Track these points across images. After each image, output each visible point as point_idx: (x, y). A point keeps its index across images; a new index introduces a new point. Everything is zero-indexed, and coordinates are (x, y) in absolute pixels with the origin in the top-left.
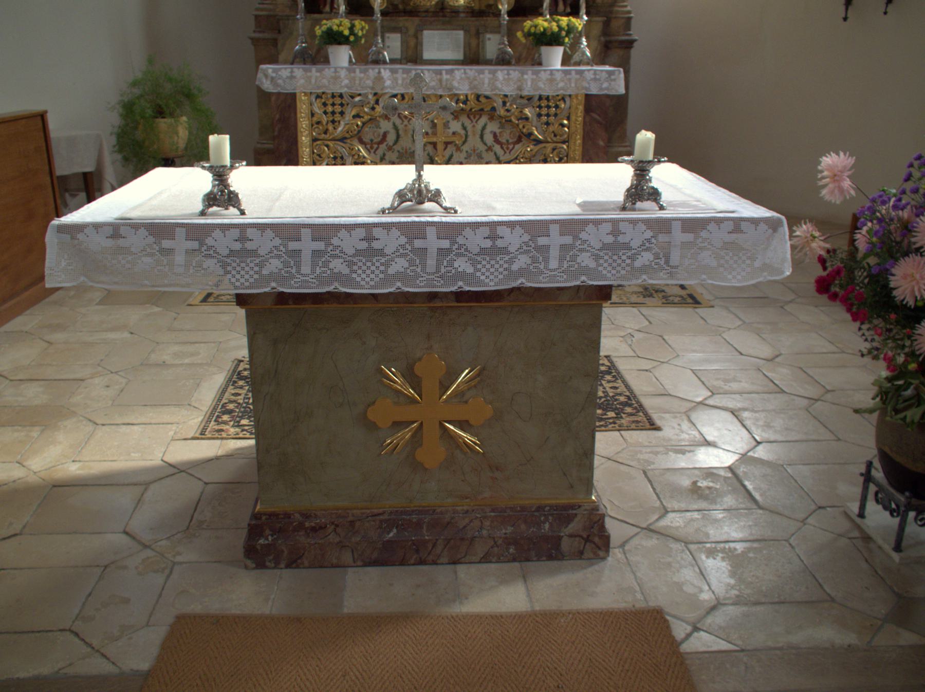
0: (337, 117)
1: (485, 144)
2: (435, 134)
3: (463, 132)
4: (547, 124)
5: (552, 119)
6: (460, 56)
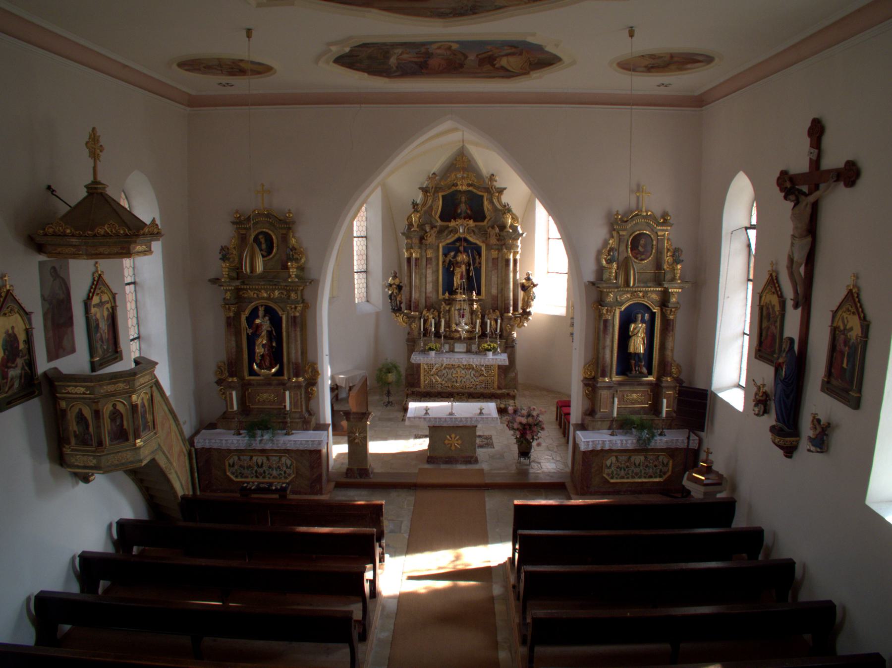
0: (431, 369)
2: (457, 374)
6: (465, 350)
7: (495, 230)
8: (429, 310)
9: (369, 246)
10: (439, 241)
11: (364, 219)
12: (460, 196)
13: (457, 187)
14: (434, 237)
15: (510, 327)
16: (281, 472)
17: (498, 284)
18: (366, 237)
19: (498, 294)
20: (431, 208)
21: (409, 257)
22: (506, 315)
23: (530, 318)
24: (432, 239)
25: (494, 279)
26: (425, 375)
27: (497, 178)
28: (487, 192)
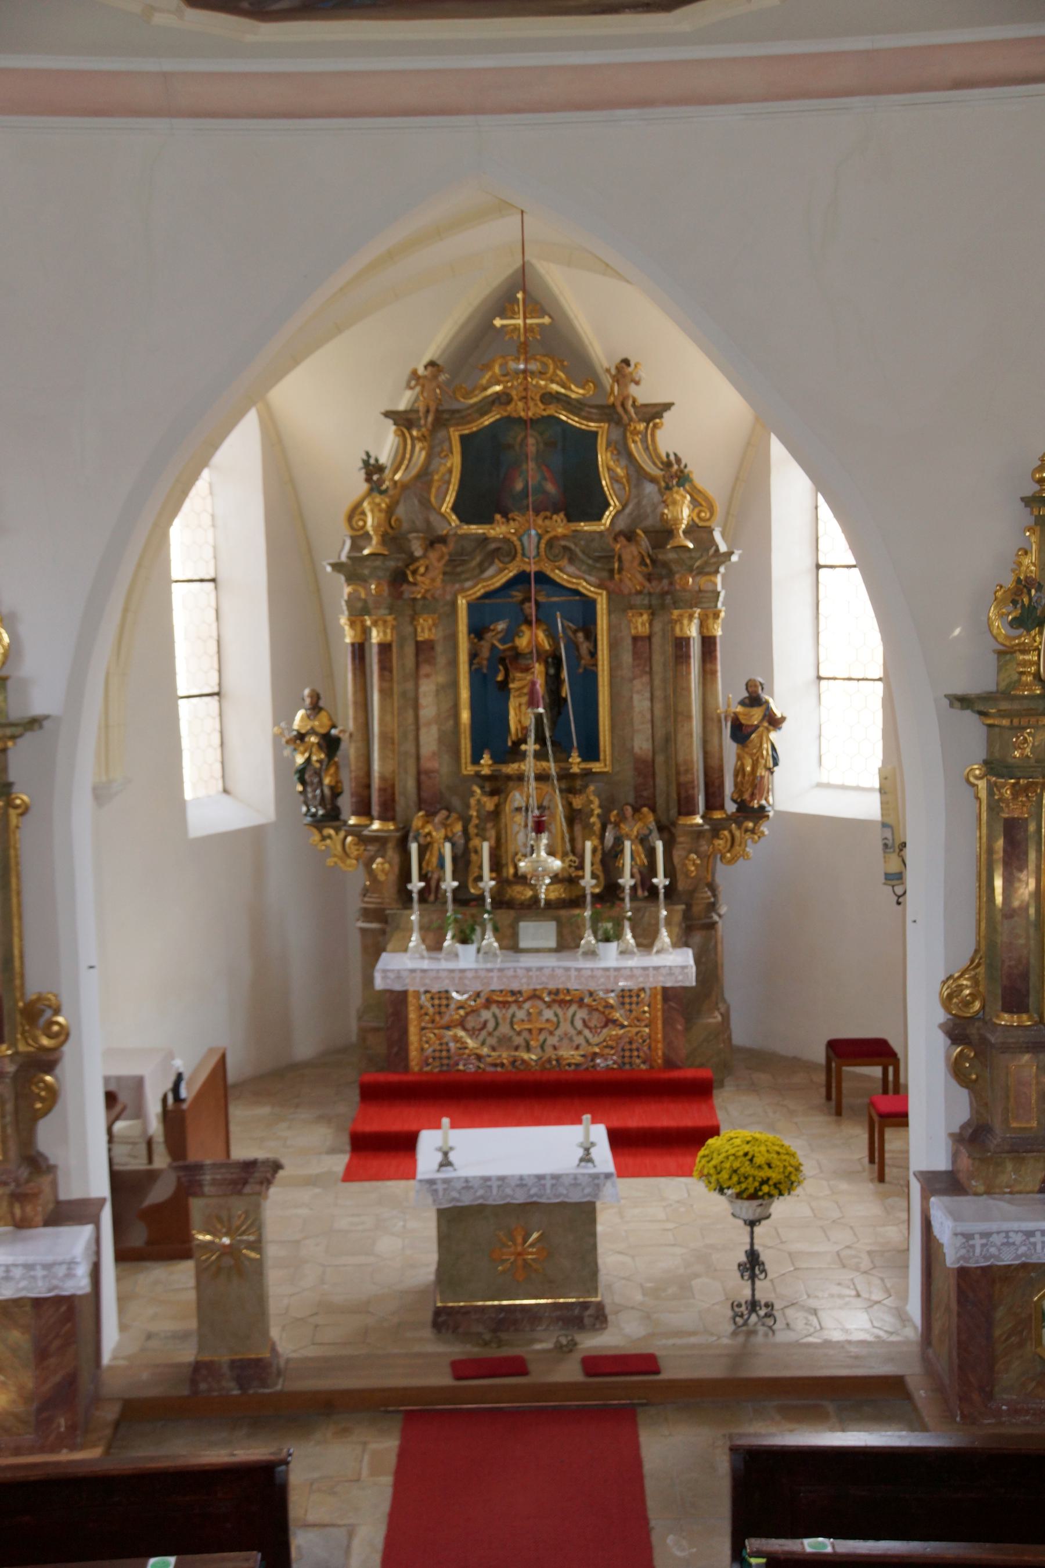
0: (443, 1009)
1: (575, 1028)
3: (555, 1019)
4: (631, 1011)
5: (634, 1006)
6: (552, 943)
7: (638, 544)
8: (430, 815)
9: (225, 608)
10: (457, 586)
11: (207, 520)
12: (522, 435)
13: (509, 408)
14: (437, 573)
15: (698, 862)
17: (652, 722)
18: (213, 580)
19: (654, 753)
20: (424, 475)
21: (358, 640)
22: (683, 821)
23: (765, 828)
24: (433, 580)
25: (641, 704)
26: (423, 1029)
27: (642, 373)
28: (609, 421)
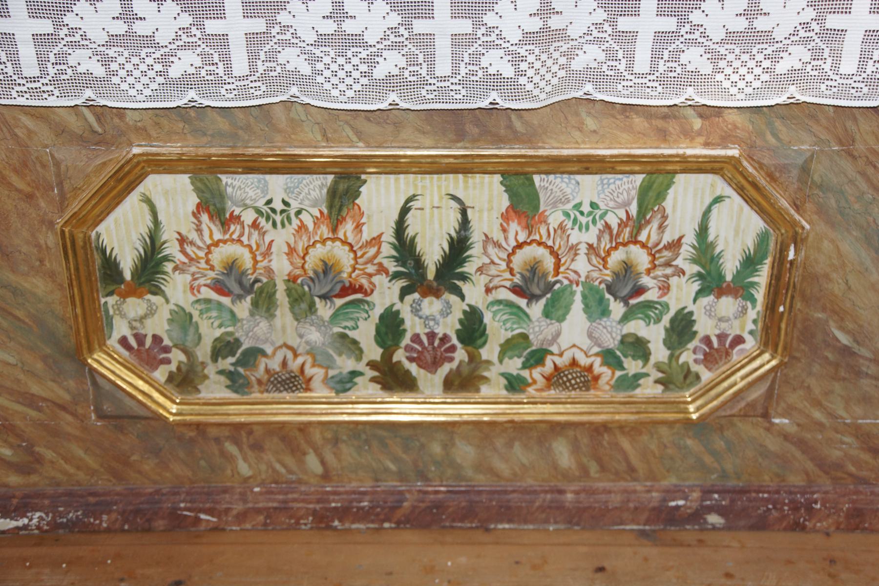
16: (637, 327)
